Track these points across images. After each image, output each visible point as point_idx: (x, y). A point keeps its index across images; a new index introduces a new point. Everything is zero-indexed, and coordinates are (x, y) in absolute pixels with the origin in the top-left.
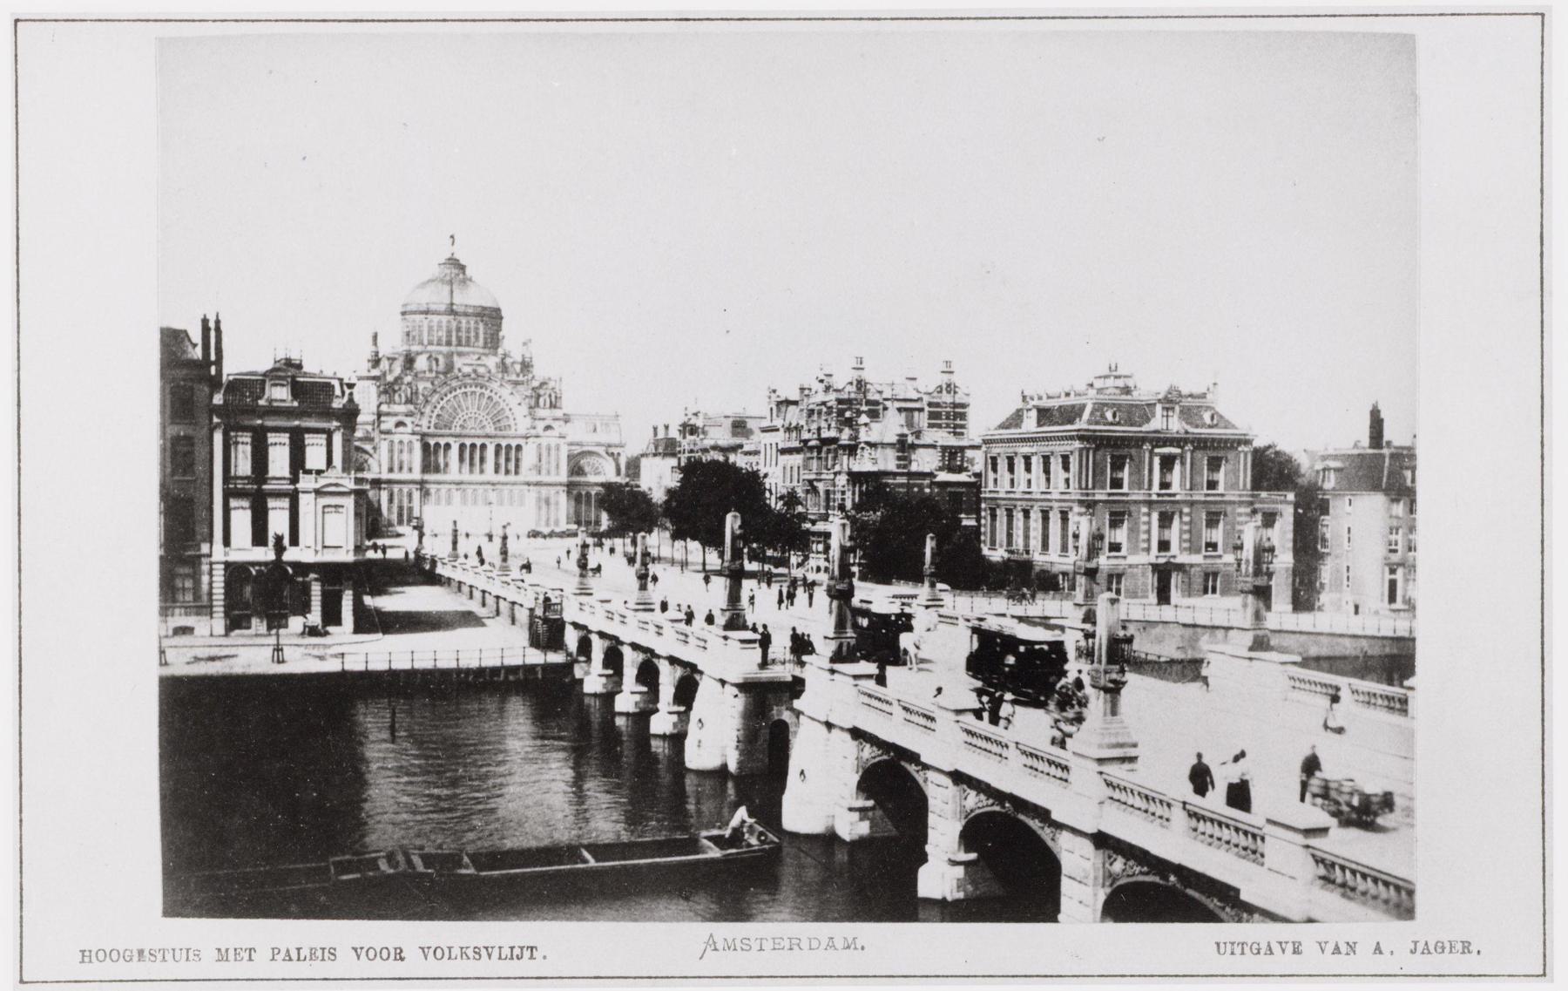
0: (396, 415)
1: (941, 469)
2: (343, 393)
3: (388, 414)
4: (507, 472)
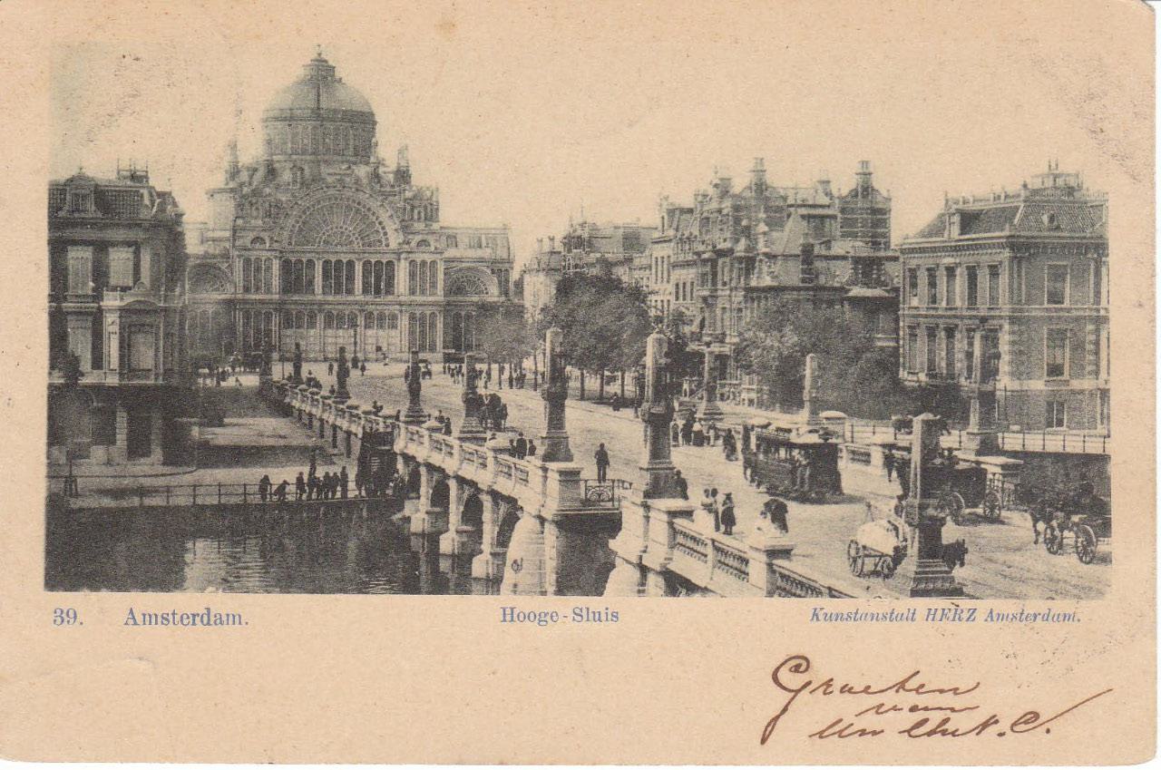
1: (854, 283)
3: (244, 229)
4: (378, 292)
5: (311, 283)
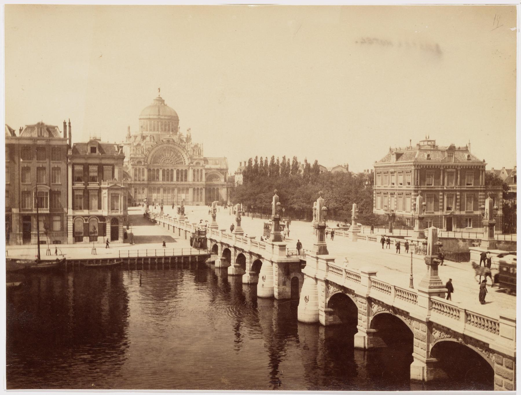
0: (137, 158)
2: (119, 150)
4: (182, 180)
5: (158, 178)
